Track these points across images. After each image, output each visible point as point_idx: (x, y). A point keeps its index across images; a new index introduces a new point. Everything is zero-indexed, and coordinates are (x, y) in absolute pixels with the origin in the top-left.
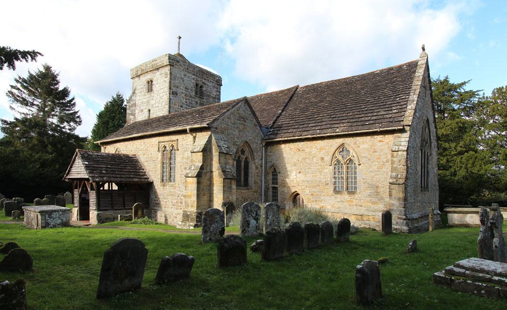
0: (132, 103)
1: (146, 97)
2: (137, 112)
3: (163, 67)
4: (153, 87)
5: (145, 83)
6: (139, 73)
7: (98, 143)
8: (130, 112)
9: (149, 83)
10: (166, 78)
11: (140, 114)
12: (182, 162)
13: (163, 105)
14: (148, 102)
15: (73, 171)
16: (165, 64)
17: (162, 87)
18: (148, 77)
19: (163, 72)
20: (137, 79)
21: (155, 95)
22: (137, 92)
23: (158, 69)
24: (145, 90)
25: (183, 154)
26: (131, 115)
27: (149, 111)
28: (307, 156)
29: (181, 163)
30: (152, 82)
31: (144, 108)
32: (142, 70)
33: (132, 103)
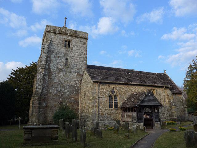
0: (50, 49)
2: (52, 56)
3: (82, 38)
5: (63, 40)
6: (58, 31)
9: (66, 41)
10: (84, 45)
13: (81, 59)
17: (80, 49)
18: (67, 38)
20: (53, 34)
21: (74, 52)
22: (53, 42)
23: (78, 37)
24: (62, 44)
27: (67, 59)
30: (69, 42)
31: (62, 56)
32: (62, 31)
33: (50, 49)
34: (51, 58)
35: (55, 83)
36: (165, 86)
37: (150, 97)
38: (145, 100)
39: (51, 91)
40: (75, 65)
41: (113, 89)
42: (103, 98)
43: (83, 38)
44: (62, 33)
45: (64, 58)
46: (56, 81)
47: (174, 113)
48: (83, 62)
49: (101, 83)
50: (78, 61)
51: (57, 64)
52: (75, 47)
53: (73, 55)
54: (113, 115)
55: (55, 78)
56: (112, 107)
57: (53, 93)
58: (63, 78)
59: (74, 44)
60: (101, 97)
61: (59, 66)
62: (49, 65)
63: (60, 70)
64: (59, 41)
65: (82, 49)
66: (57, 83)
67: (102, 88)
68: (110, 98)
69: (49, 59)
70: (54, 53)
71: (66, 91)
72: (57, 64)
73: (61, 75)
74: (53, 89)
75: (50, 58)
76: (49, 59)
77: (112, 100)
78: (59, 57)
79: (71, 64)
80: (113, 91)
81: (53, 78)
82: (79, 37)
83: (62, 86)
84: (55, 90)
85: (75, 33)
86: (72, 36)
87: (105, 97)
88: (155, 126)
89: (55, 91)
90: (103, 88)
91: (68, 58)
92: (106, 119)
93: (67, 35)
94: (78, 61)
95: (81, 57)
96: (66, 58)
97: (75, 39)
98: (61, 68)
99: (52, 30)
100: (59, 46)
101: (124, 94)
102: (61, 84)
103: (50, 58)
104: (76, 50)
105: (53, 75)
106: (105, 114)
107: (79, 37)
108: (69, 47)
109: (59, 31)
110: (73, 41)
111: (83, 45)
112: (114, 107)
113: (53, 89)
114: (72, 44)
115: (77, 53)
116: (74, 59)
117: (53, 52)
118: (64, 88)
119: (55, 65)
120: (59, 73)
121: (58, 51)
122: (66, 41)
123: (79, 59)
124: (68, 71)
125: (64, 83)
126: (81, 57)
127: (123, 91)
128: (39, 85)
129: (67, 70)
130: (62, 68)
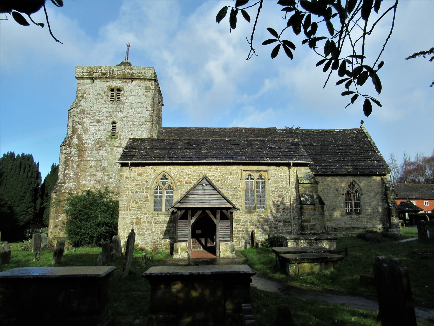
1: (106, 106)
2: (86, 120)
4: (123, 98)
7: (128, 163)
8: (78, 120)
11: (93, 124)
12: (275, 191)
14: (111, 113)
15: (188, 199)
16: (148, 78)
19: (142, 85)
20: (89, 81)
25: (275, 183)
26: (79, 124)
28: (325, 187)
29: (274, 191)
30: (119, 90)
31: (105, 118)
32: (103, 74)
34: (85, 125)
35: (91, 167)
36: (292, 162)
37: (204, 190)
38: (191, 197)
39: (84, 182)
40: (128, 131)
41: (164, 176)
42: (140, 192)
43: (144, 79)
44: (103, 76)
45: (107, 122)
46: (93, 164)
47: (309, 221)
48: (145, 124)
49: (133, 165)
50: (135, 123)
51: (96, 134)
52: (129, 98)
53: (124, 115)
54: (161, 225)
55: (92, 158)
56: (161, 210)
57: (87, 185)
58: (106, 157)
59: (126, 94)
60: (137, 192)
61: (99, 137)
62: (79, 138)
63: (100, 145)
64: (98, 92)
65: (143, 100)
66: (95, 167)
67: (140, 175)
68: (156, 193)
69: (79, 126)
70: (90, 116)
71: (111, 180)
72: (96, 134)
73: (103, 153)
74: (89, 178)
75: (82, 125)
76: (79, 126)
77: (161, 197)
78: (98, 121)
79: (122, 131)
80: (164, 178)
81: (89, 159)
82: (137, 79)
83: (104, 172)
84: (91, 180)
85: (129, 72)
86: (124, 78)
87: (145, 190)
88: (219, 249)
89: (92, 182)
90: (143, 173)
91: (116, 120)
92: (146, 231)
93: (112, 78)
94: (135, 123)
95: (140, 116)
96: (111, 121)
97: (129, 84)
98: (103, 140)
99: (84, 74)
100: (100, 100)
101: (186, 183)
102: (103, 169)
103: (82, 125)
104: (133, 103)
105: (88, 154)
106: (144, 222)
107: (137, 79)
108: (119, 100)
109: (98, 74)
110: (124, 88)
111: (145, 93)
112: (164, 210)
113: (89, 178)
114: (123, 95)
115: (133, 110)
116: (128, 121)
117: (89, 114)
118: (108, 175)
119: (91, 136)
120: (99, 149)
121: (98, 110)
122: (112, 90)
123: (135, 120)
124: (116, 144)
125: (107, 166)
126: (140, 116)
127: (185, 178)
128: (61, 173)
129: (113, 144)
130: (104, 140)
